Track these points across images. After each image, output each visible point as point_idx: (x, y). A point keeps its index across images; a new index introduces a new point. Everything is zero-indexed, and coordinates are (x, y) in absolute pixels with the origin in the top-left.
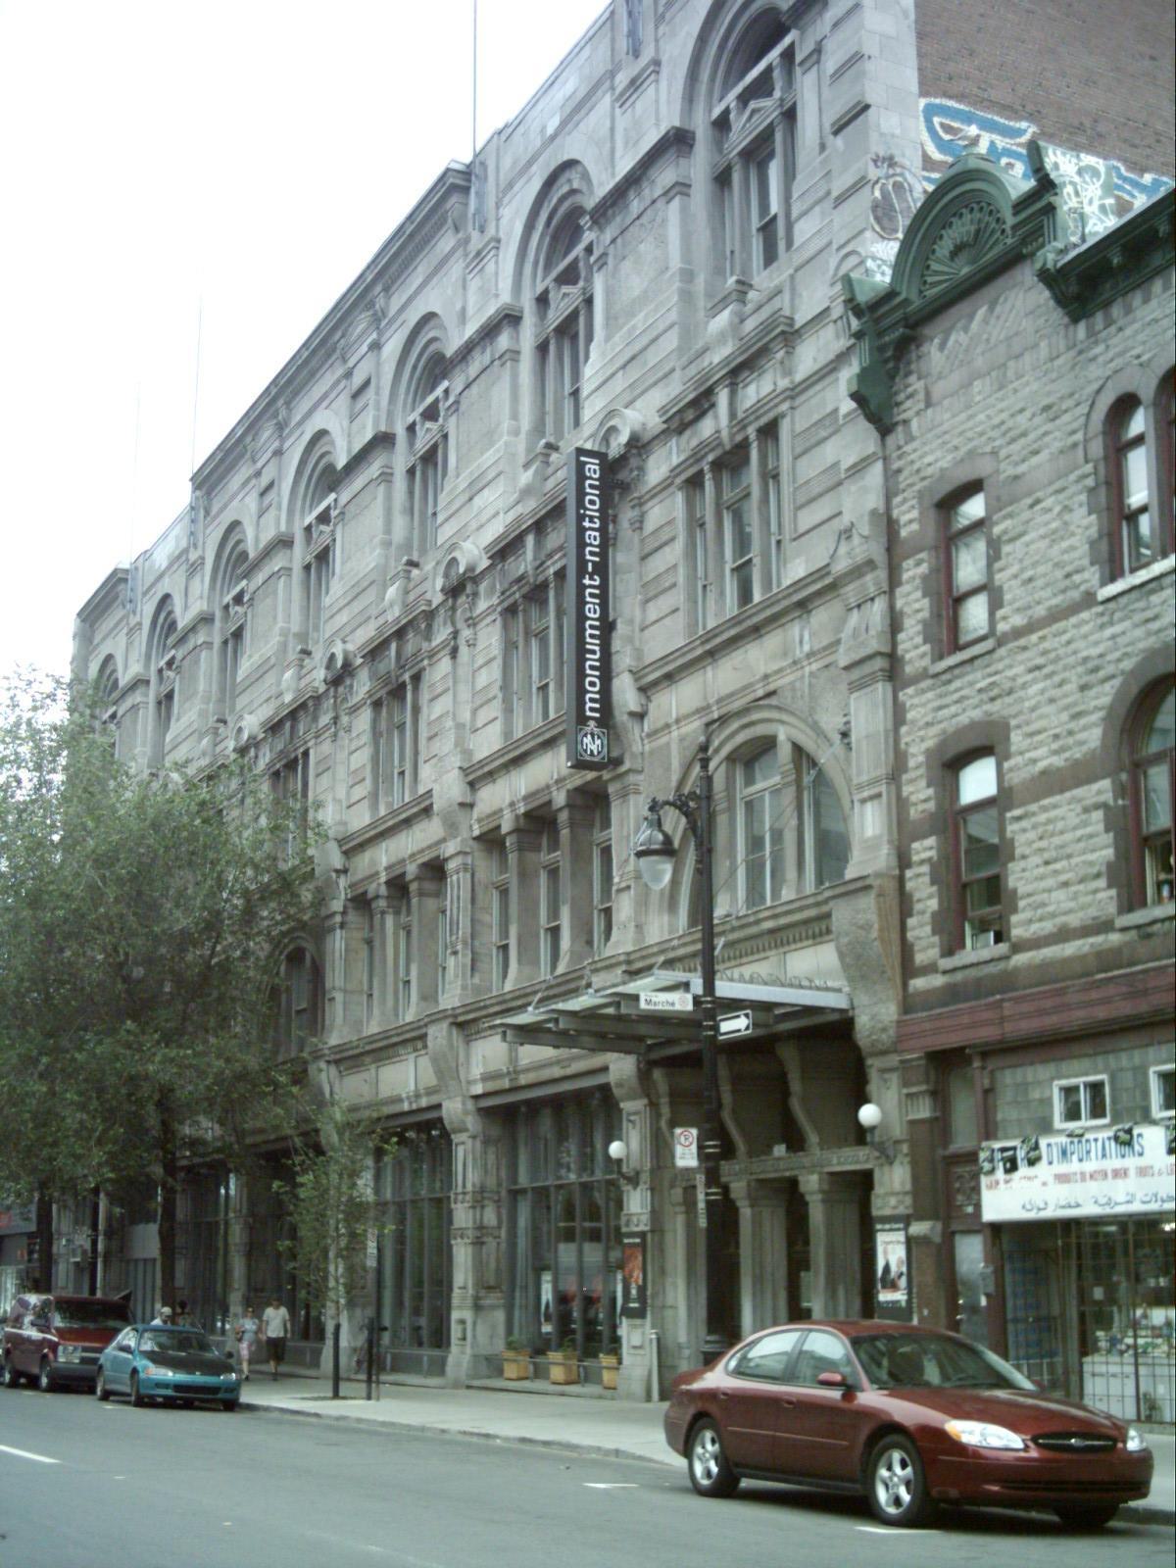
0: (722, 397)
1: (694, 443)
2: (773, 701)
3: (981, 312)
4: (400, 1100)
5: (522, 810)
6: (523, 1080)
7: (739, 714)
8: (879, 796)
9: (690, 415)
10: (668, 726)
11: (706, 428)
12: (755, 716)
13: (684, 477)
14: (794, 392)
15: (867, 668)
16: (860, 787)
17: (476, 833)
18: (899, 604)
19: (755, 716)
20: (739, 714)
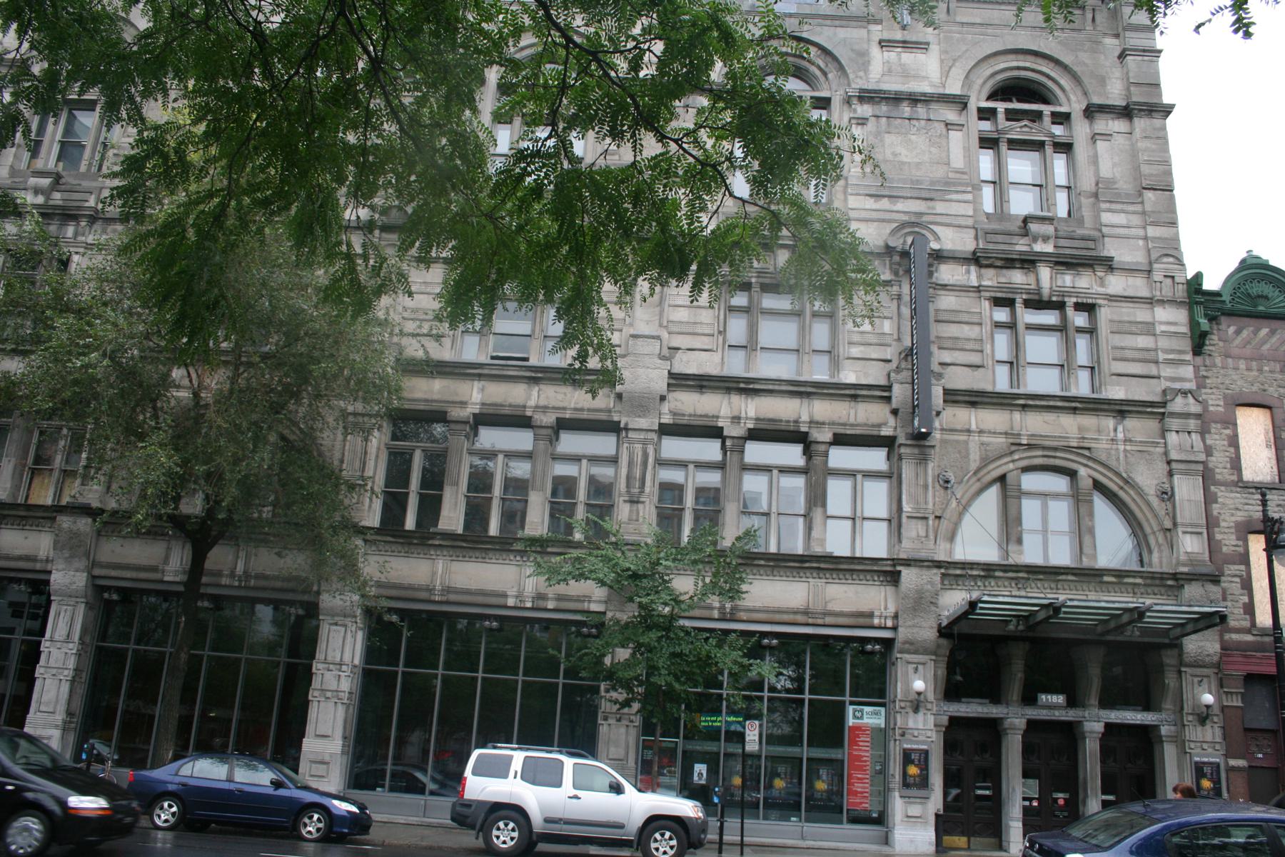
0: (1045, 272)
1: (1003, 280)
2: (1086, 453)
3: (1264, 331)
4: (505, 596)
5: (751, 426)
6: (743, 616)
7: (1044, 448)
8: (1200, 533)
9: (999, 263)
10: (969, 431)
11: (1018, 277)
12: (1058, 454)
13: (993, 294)
14: (1112, 298)
15: (1193, 466)
16: (1183, 525)
17: (667, 419)
18: (1209, 442)
19: (1058, 454)
20: (1044, 448)
